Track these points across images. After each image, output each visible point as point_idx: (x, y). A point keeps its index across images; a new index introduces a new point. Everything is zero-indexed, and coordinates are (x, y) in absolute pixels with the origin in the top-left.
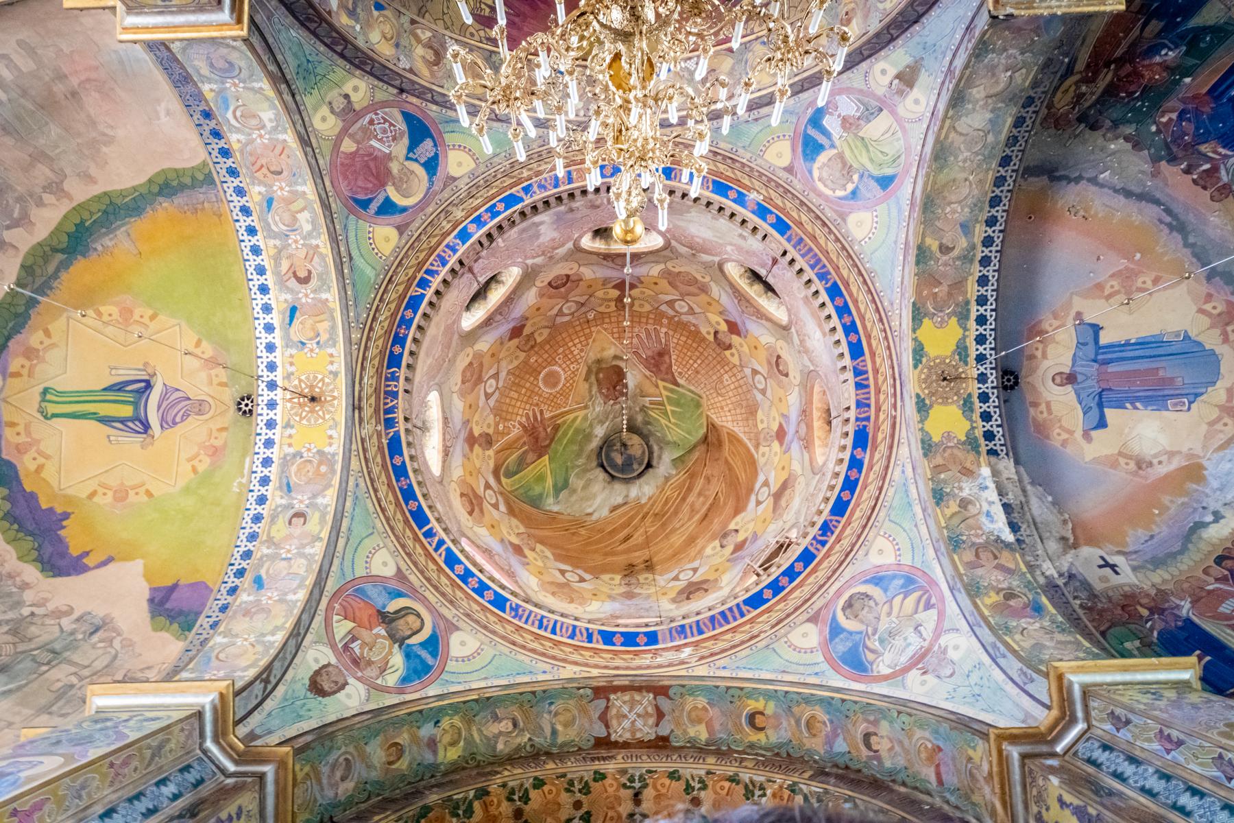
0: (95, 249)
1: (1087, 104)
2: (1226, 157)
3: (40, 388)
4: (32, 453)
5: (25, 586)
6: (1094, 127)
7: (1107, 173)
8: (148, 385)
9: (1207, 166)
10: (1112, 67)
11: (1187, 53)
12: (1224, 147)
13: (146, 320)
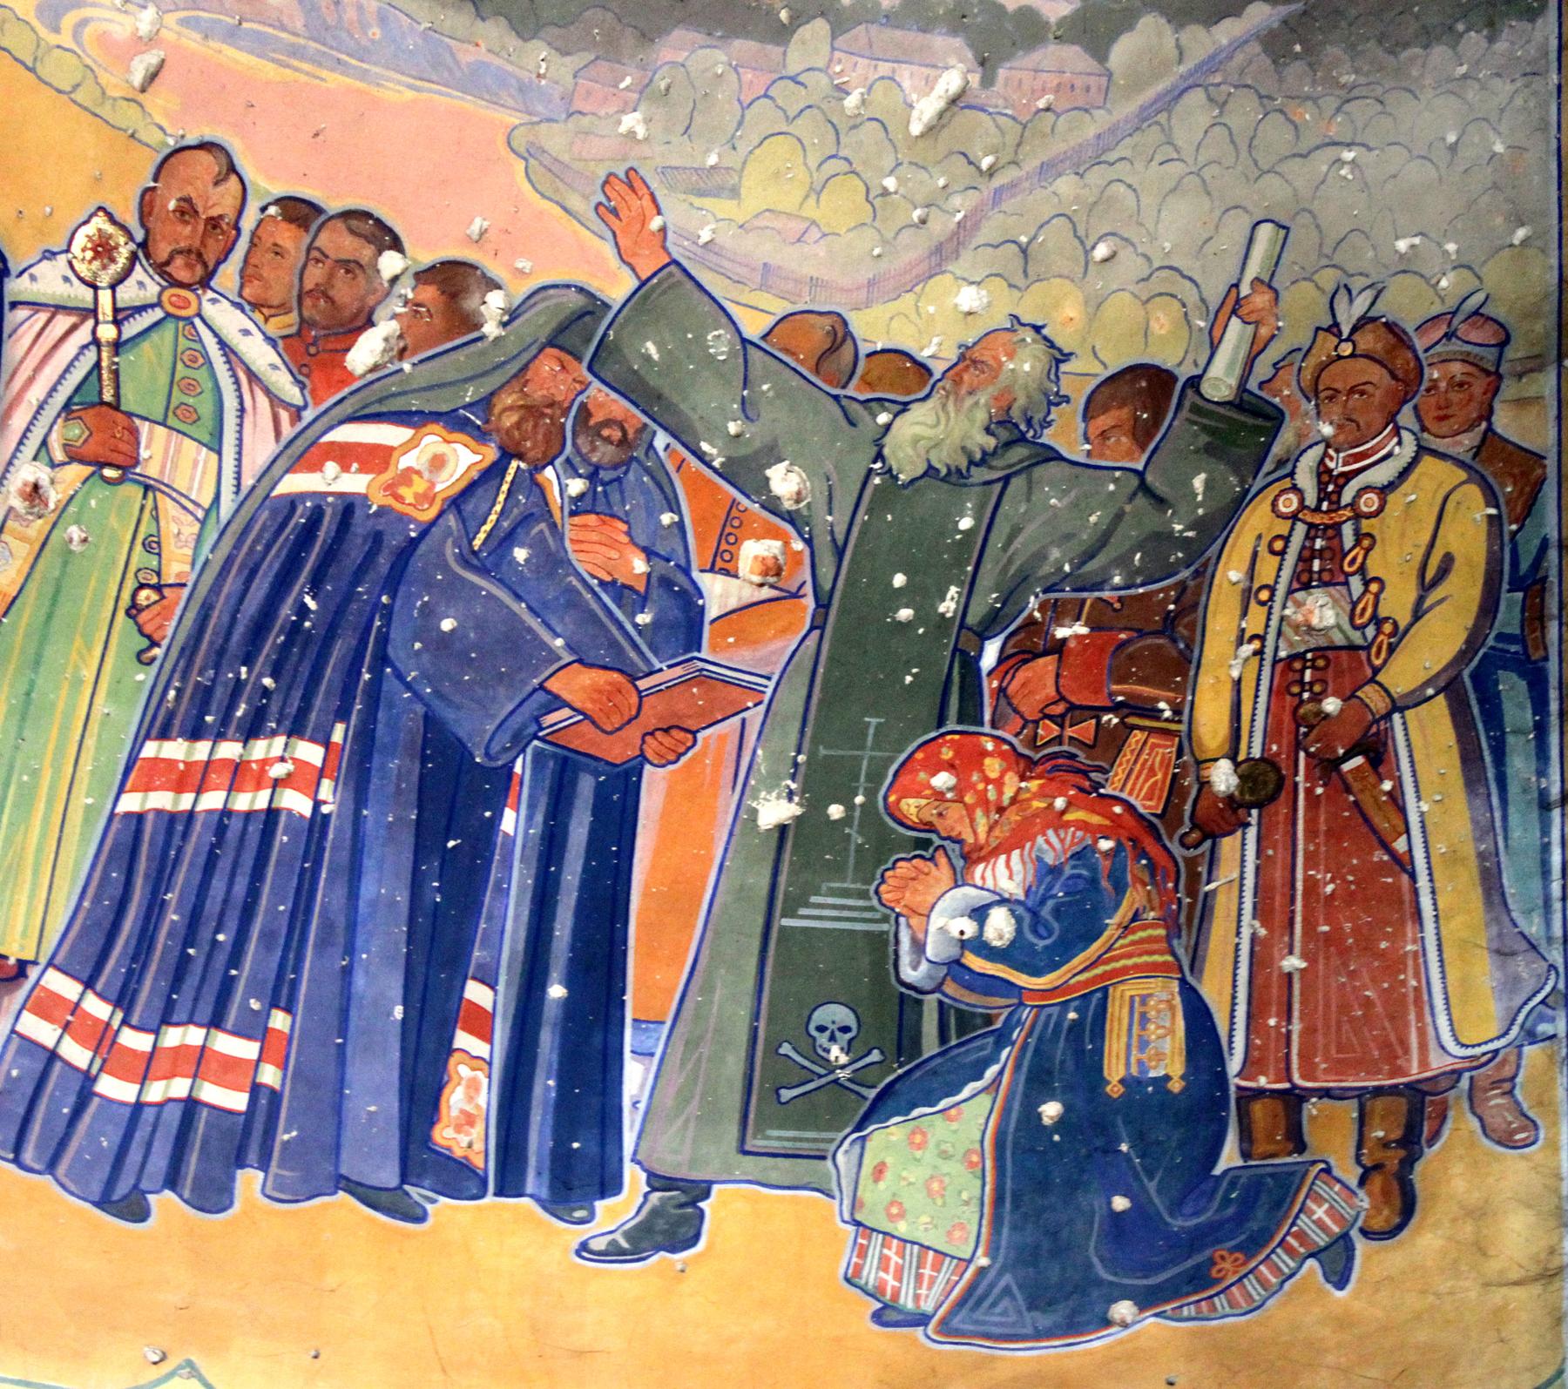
1: (1257, 521)
2: (305, 454)
6: (1146, 390)
7: (927, 108)
9: (365, 353)
10: (1223, 777)
11: (881, 948)
12: (349, 506)
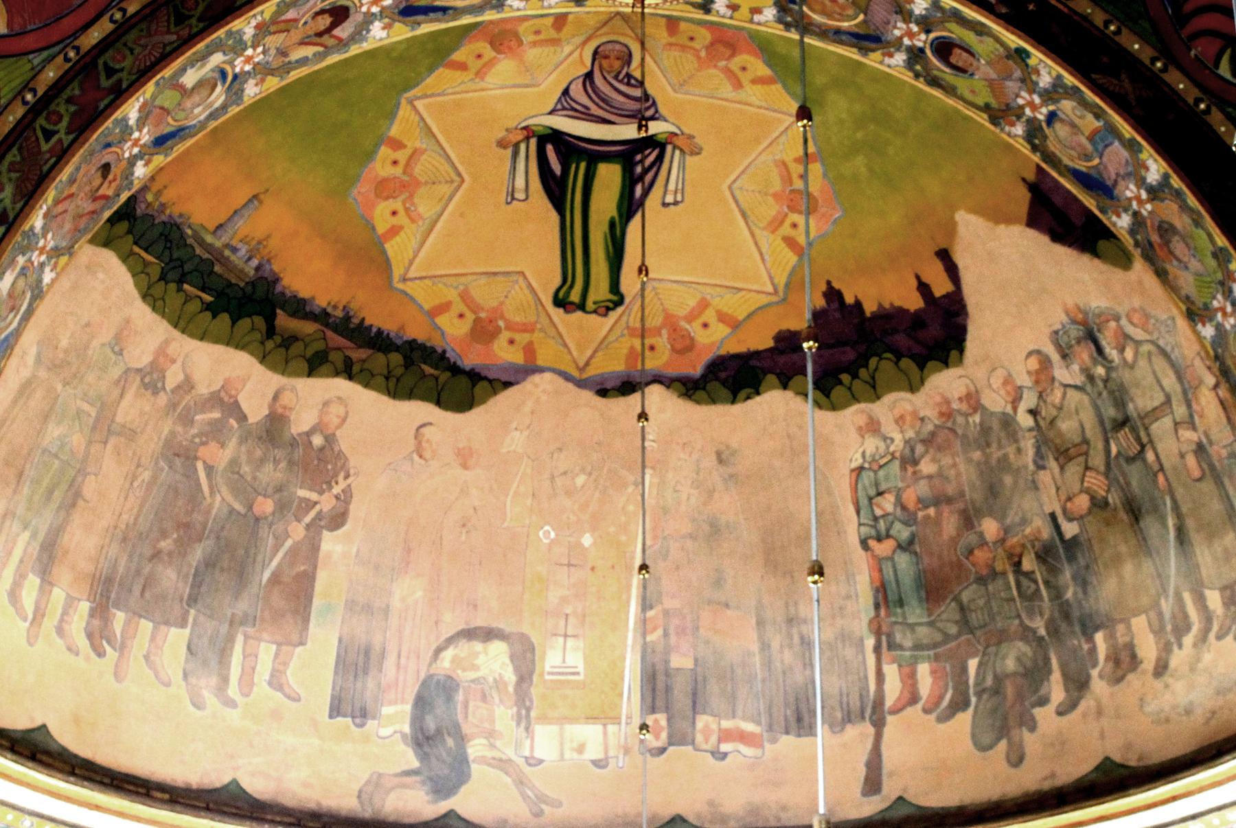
0: (258, 269)
3: (557, 314)
4: (695, 329)
5: (973, 400)
8: (555, 137)
13: (402, 156)
